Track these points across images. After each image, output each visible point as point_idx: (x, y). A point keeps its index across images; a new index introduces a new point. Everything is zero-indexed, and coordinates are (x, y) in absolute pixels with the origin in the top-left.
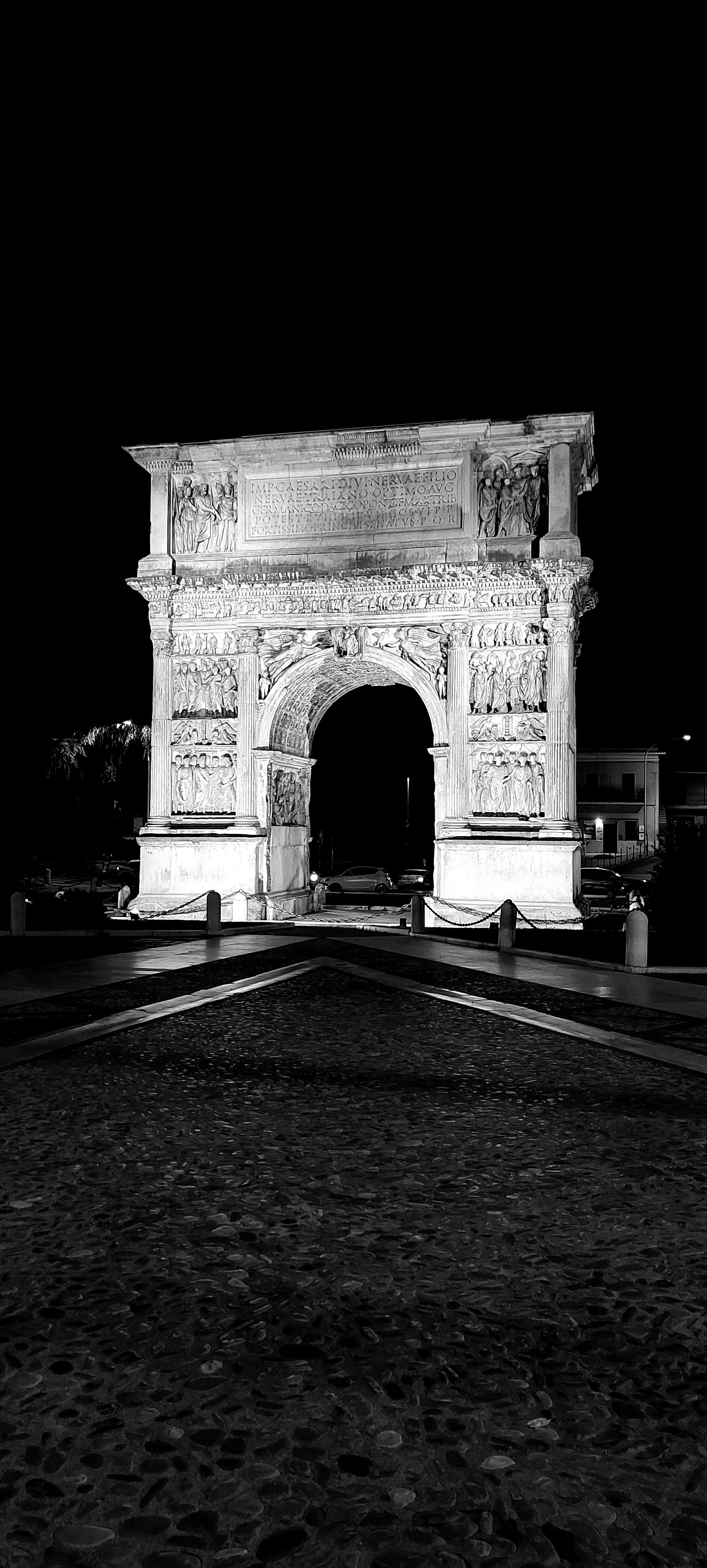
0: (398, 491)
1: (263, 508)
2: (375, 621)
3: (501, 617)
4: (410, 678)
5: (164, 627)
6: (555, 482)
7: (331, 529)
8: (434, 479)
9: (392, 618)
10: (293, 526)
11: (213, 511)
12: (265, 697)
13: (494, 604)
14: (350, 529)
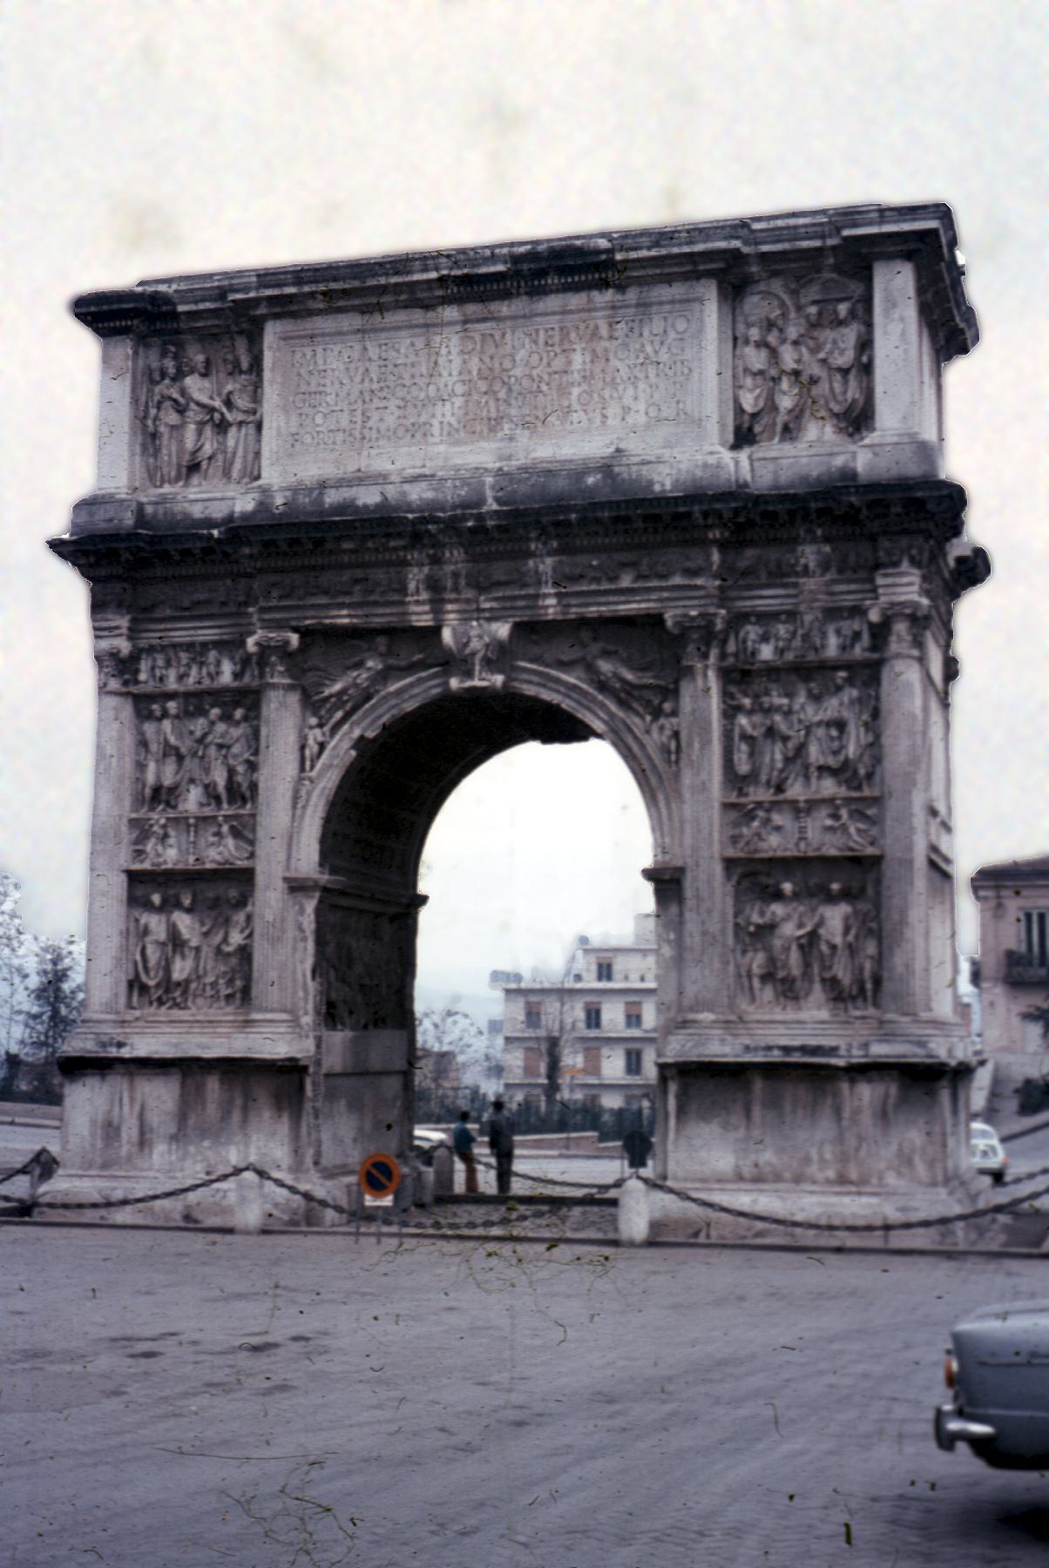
0: (578, 359)
6: (886, 333)
11: (217, 403)
12: (312, 767)
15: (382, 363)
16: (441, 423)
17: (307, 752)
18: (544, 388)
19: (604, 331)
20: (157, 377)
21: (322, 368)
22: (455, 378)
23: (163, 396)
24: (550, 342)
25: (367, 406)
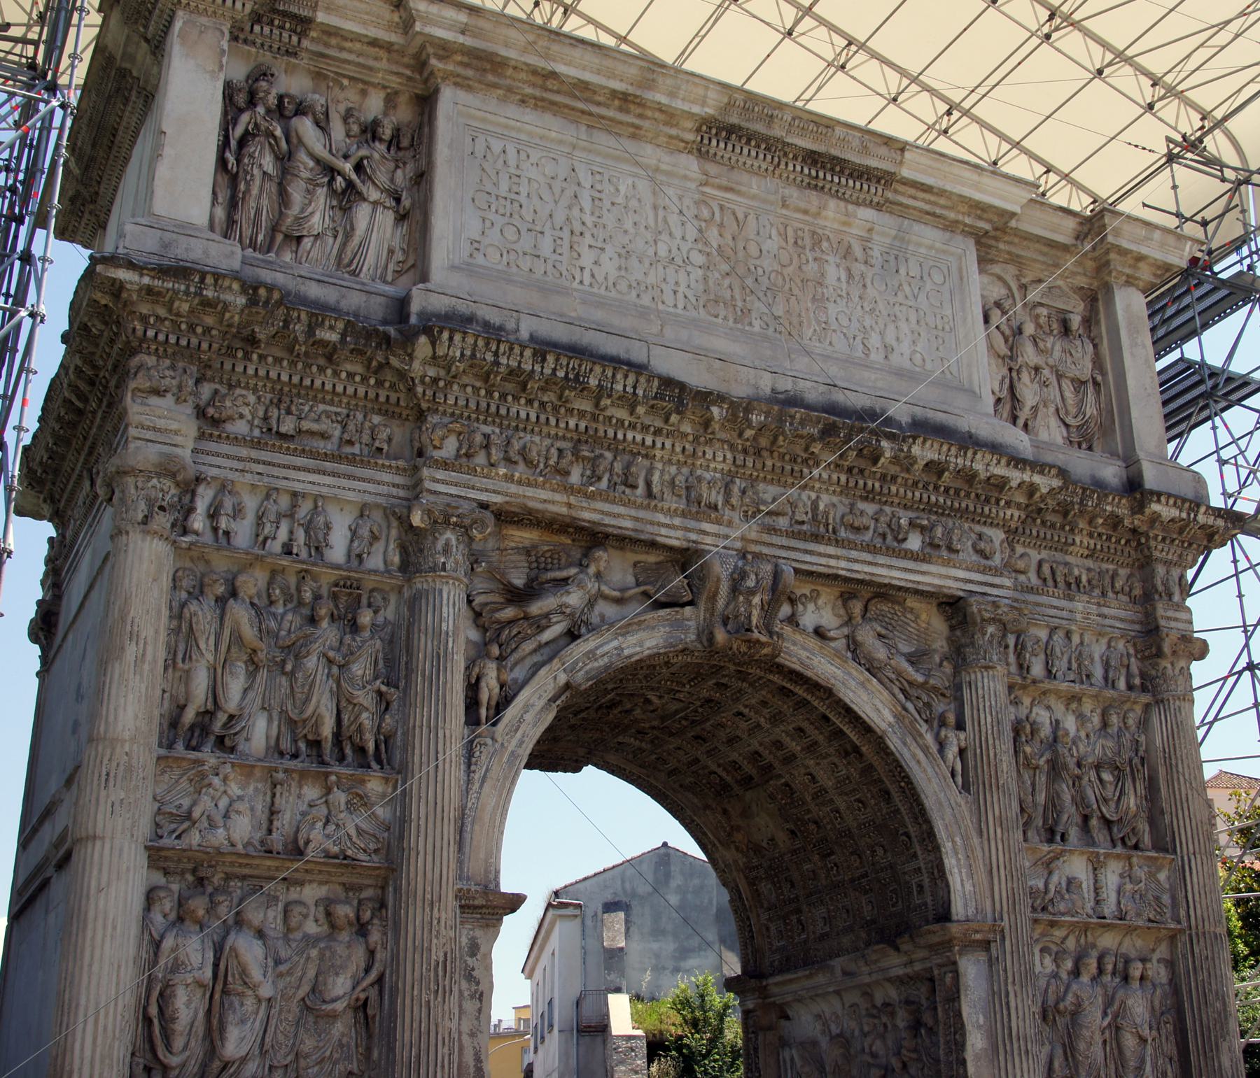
1: (502, 201)
2: (808, 558)
3: (1059, 613)
4: (883, 726)
5: (179, 440)
6: (1132, 354)
7: (680, 306)
8: (903, 271)
9: (849, 560)
10: (582, 269)
11: (348, 167)
13: (1045, 580)
14: (725, 318)
15: (597, 195)
16: (675, 292)
17: (484, 696)
18: (796, 291)
19: (858, 251)
20: (241, 99)
21: (512, 170)
22: (690, 245)
23: (256, 125)
24: (800, 242)
25: (575, 239)
